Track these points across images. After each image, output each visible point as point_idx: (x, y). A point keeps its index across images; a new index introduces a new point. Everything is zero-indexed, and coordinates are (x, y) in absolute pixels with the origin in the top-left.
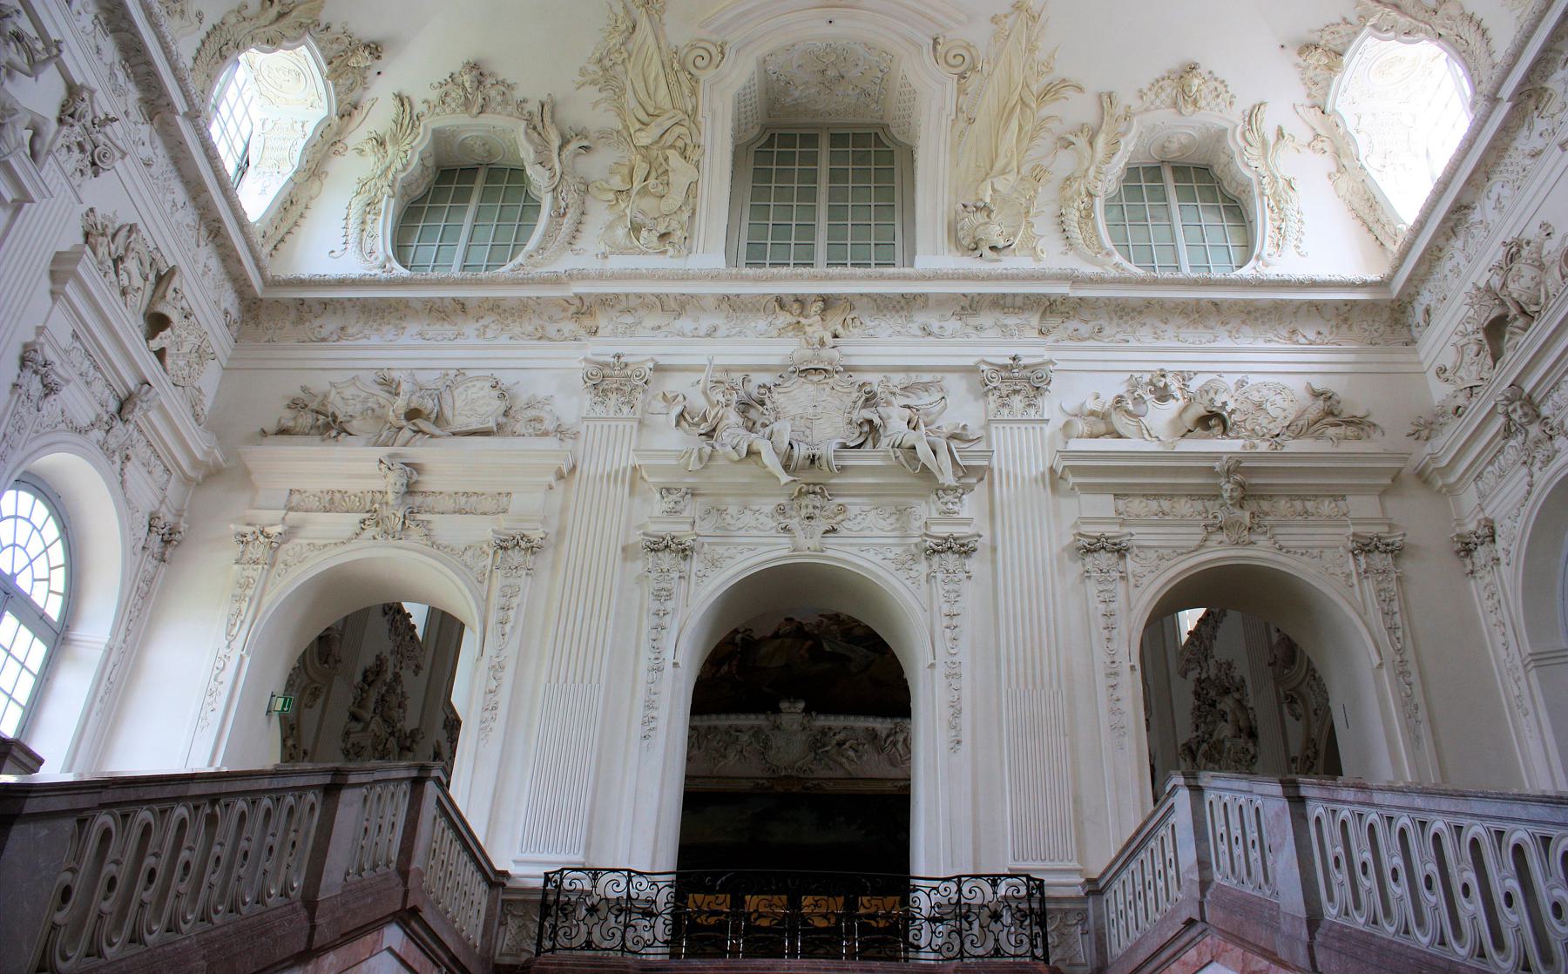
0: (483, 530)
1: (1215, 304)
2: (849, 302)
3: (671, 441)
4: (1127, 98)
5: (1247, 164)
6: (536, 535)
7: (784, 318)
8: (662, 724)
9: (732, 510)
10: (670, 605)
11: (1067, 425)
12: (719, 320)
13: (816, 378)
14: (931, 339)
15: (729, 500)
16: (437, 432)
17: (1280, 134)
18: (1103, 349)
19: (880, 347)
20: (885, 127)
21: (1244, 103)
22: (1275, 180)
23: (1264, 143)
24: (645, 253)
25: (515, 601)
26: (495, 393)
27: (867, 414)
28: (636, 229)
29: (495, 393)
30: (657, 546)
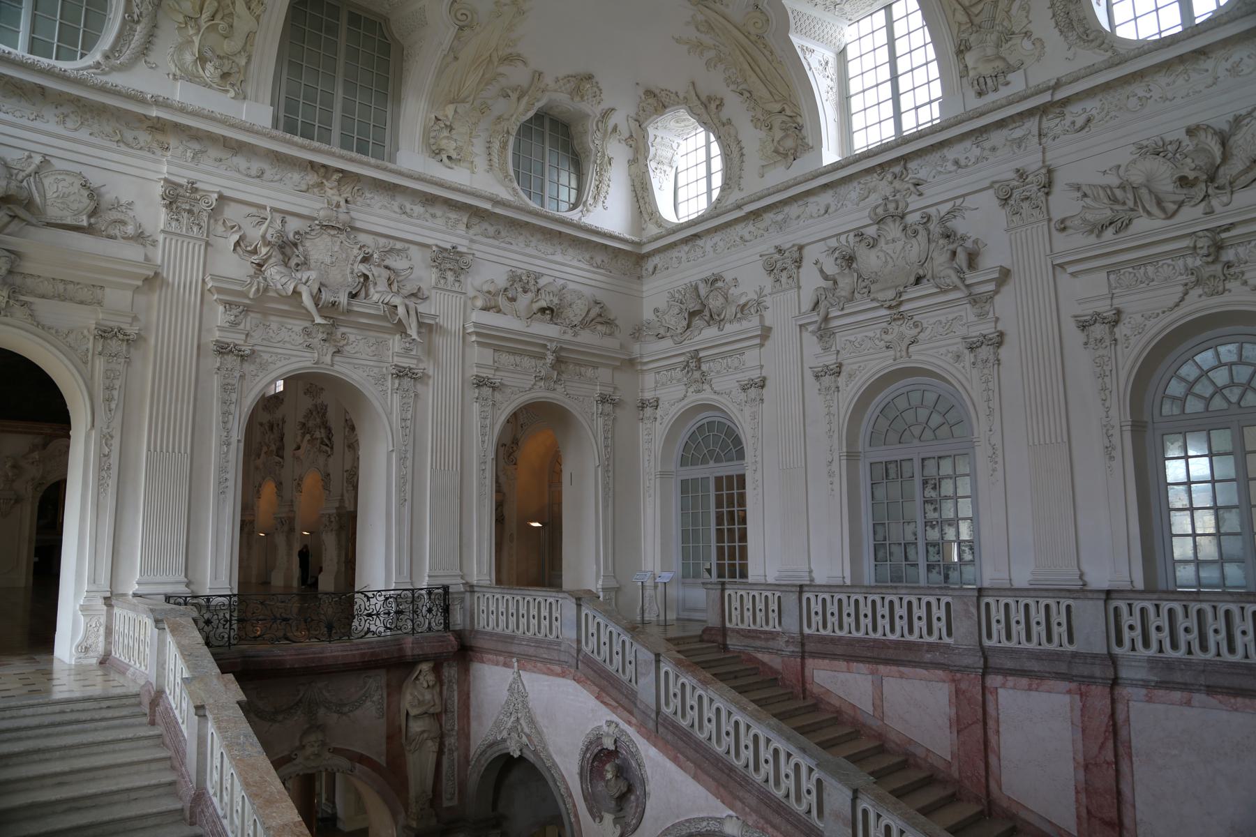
0: (87, 319)
1: (560, 233)
2: (358, 178)
3: (234, 267)
4: (549, 80)
5: (593, 140)
6: (132, 330)
7: (312, 178)
8: (231, 483)
9: (274, 326)
10: (234, 396)
11: (475, 297)
12: (266, 166)
13: (333, 232)
14: (404, 217)
15: (272, 318)
16: (34, 221)
17: (615, 129)
18: (498, 248)
19: (377, 217)
20: (386, 20)
21: (605, 105)
22: (603, 155)
23: (606, 130)
24: (210, 87)
25: (117, 383)
26: (86, 193)
27: (363, 268)
28: (202, 59)
29: (86, 193)
30: (223, 349)
